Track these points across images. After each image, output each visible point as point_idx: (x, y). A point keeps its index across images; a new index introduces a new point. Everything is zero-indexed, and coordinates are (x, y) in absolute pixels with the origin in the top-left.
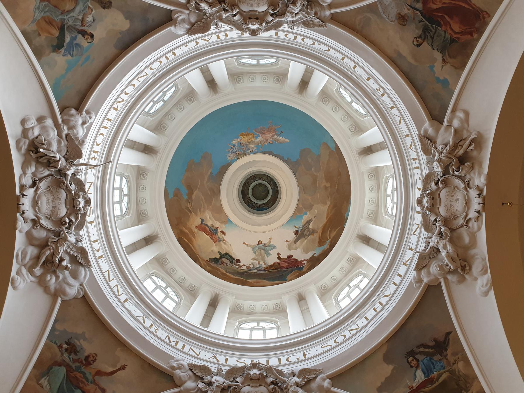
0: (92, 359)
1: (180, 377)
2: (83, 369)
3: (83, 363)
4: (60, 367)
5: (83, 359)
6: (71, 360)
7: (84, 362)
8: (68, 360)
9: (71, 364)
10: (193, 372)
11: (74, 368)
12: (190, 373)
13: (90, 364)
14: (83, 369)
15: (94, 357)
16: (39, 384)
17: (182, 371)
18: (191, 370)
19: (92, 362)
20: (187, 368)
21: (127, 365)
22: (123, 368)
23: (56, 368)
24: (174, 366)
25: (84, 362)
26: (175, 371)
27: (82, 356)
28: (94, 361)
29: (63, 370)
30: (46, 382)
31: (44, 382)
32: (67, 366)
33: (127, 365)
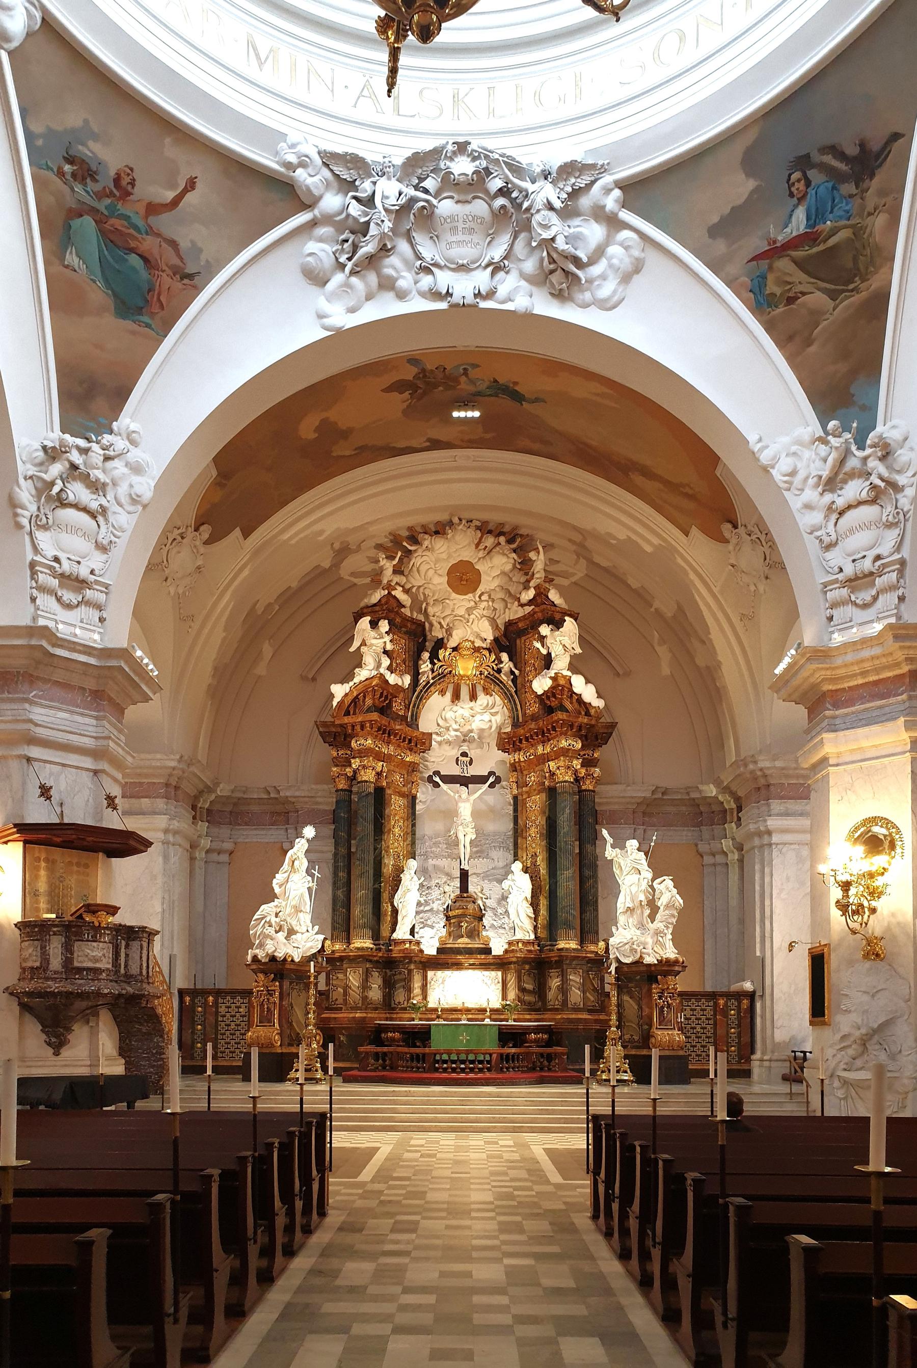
0: (127, 179)
1: (308, 189)
2: (121, 208)
3: (115, 196)
4: (81, 219)
5: (112, 186)
6: (90, 196)
7: (118, 194)
8: (88, 199)
9: (95, 204)
10: (332, 171)
11: (106, 213)
12: (326, 173)
13: (129, 194)
14: (121, 208)
15: (128, 175)
16: (67, 267)
17: (310, 170)
18: (326, 165)
19: (129, 188)
20: (318, 161)
21: (196, 178)
22: (191, 185)
23: (76, 223)
24: (290, 163)
25: (118, 194)
26: (294, 172)
27: (106, 181)
28: (133, 183)
29: (87, 223)
30: (76, 260)
31: (72, 258)
32: (93, 211)
33: (196, 178)
